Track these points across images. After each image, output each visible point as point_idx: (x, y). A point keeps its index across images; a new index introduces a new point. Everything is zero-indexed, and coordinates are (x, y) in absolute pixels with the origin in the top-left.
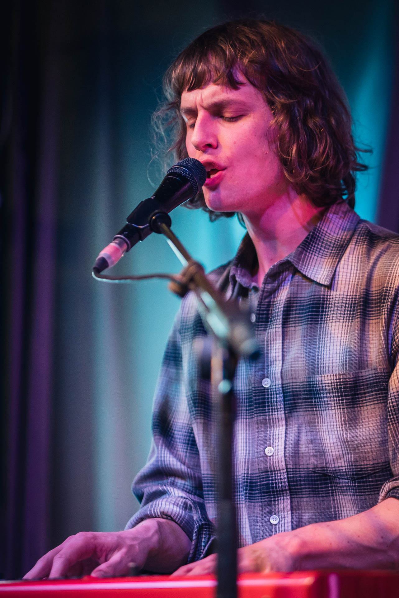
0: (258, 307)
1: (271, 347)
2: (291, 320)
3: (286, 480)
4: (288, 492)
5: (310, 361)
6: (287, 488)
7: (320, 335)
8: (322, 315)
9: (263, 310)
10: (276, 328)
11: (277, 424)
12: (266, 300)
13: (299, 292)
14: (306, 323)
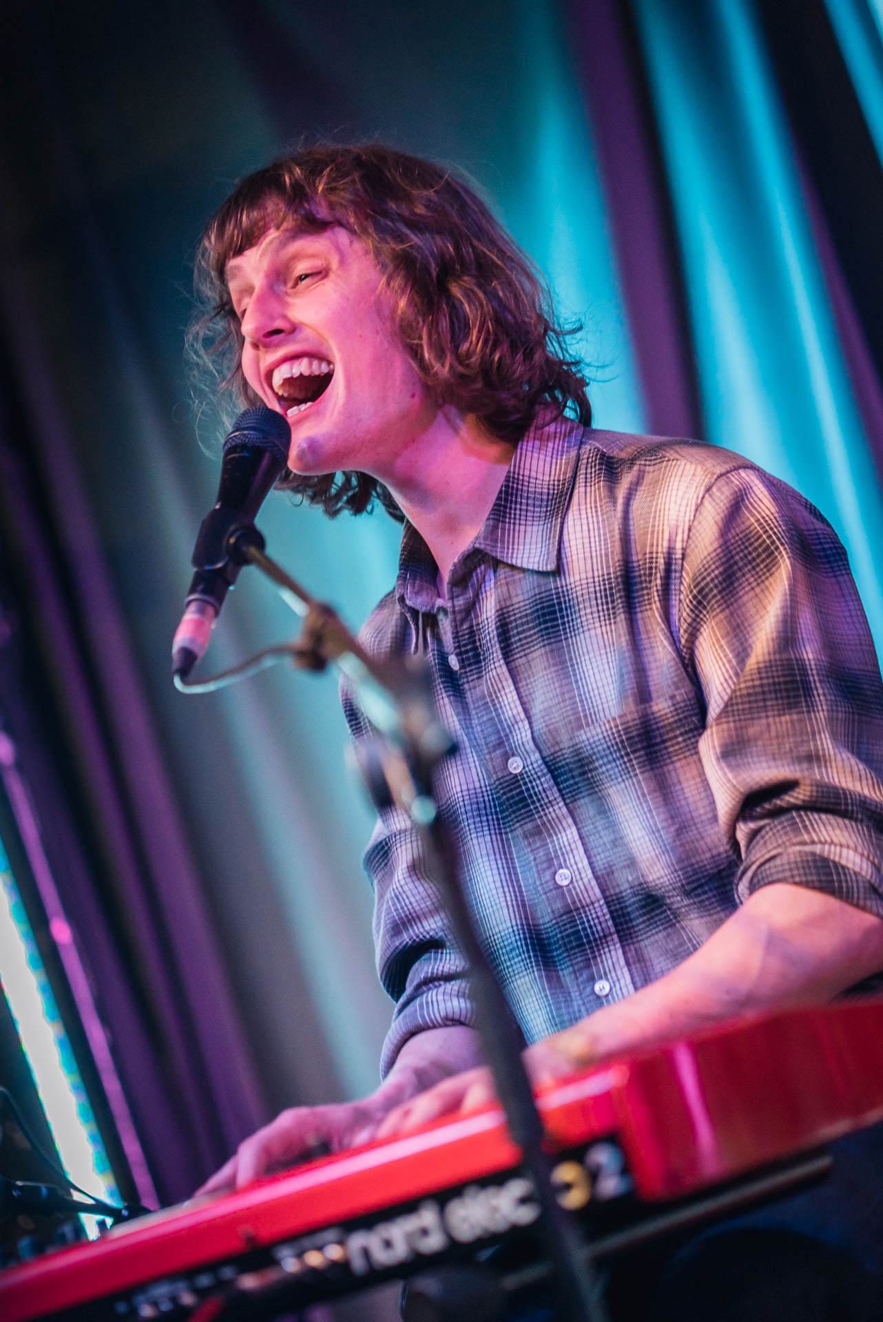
0: (454, 643)
1: (499, 702)
2: (515, 646)
3: (608, 916)
4: (615, 936)
5: (569, 708)
6: (613, 930)
7: (571, 659)
8: (564, 624)
9: (465, 645)
10: (496, 667)
11: (560, 827)
12: (465, 627)
13: (513, 594)
14: (542, 644)
